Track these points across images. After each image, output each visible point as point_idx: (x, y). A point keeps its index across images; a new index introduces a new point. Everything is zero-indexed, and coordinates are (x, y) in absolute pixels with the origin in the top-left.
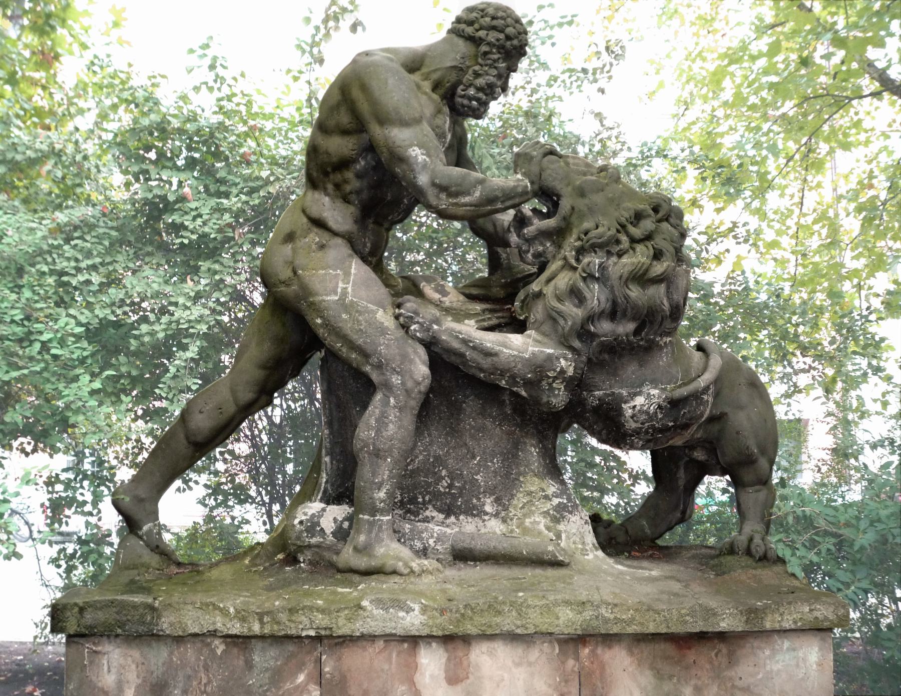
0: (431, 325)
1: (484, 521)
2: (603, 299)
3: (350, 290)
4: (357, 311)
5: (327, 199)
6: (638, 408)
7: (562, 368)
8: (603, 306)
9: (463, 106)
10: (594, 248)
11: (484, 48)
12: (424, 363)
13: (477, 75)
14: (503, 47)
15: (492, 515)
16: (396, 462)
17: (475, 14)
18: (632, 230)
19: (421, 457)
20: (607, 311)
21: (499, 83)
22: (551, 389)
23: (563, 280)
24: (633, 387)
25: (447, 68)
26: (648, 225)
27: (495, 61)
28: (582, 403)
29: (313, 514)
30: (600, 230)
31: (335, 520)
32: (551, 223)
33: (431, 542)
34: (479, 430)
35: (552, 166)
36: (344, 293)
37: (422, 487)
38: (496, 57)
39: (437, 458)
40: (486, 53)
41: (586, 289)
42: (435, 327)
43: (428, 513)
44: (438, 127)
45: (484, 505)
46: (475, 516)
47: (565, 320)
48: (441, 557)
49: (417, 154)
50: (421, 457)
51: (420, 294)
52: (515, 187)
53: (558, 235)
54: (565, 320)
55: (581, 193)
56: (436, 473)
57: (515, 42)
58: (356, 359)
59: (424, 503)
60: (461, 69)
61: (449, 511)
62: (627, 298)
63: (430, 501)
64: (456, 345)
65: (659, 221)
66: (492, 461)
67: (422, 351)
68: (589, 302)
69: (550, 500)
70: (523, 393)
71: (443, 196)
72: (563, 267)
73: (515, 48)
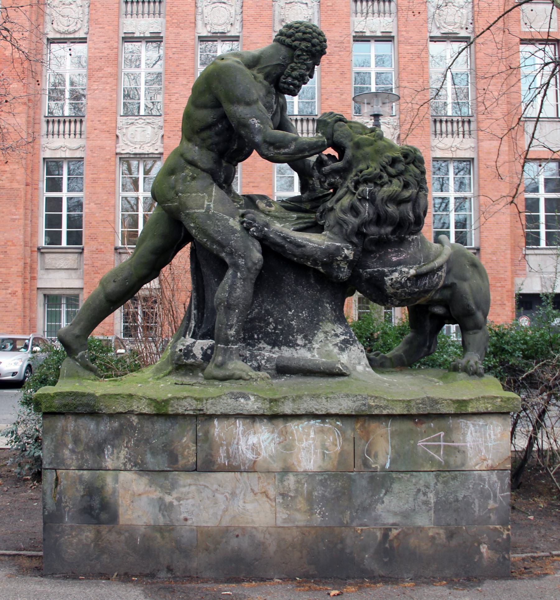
0: (263, 228)
1: (296, 350)
2: (371, 212)
3: (212, 206)
4: (217, 219)
5: (197, 148)
6: (394, 279)
7: (345, 254)
8: (371, 216)
9: (284, 88)
10: (366, 181)
11: (298, 52)
12: (258, 251)
13: (293, 69)
14: (311, 51)
15: (301, 346)
16: (241, 312)
17: (292, 31)
18: (390, 170)
19: (256, 310)
20: (374, 220)
21: (308, 73)
22: (339, 268)
23: (346, 201)
24: (391, 267)
25: (274, 65)
26: (401, 167)
27: (305, 60)
28: (360, 276)
29: (188, 345)
30: (370, 170)
31: (202, 348)
32: (339, 164)
33: (263, 362)
34: (294, 294)
35: (340, 129)
36: (208, 208)
37: (257, 329)
38: (305, 57)
39: (267, 311)
40: (299, 56)
41: (361, 206)
42: (266, 229)
43: (261, 345)
44: (268, 102)
45: (296, 340)
46: (291, 347)
47: (347, 225)
48: (270, 371)
49: (255, 123)
50: (256, 310)
51: (256, 207)
52: (317, 142)
53: (343, 172)
54: (347, 225)
55: (358, 146)
56: (266, 320)
57: (318, 48)
58: (216, 248)
59: (258, 339)
60: (283, 65)
61: (274, 344)
62: (386, 212)
63: (262, 338)
64: (279, 240)
65: (408, 164)
66: (302, 313)
67: (257, 244)
68: (363, 214)
69: (339, 337)
70: (322, 270)
71: (271, 148)
72: (346, 193)
73: (318, 51)
